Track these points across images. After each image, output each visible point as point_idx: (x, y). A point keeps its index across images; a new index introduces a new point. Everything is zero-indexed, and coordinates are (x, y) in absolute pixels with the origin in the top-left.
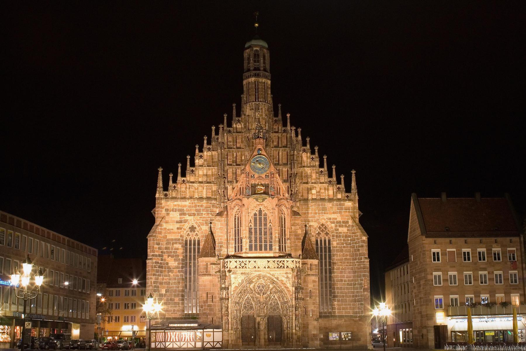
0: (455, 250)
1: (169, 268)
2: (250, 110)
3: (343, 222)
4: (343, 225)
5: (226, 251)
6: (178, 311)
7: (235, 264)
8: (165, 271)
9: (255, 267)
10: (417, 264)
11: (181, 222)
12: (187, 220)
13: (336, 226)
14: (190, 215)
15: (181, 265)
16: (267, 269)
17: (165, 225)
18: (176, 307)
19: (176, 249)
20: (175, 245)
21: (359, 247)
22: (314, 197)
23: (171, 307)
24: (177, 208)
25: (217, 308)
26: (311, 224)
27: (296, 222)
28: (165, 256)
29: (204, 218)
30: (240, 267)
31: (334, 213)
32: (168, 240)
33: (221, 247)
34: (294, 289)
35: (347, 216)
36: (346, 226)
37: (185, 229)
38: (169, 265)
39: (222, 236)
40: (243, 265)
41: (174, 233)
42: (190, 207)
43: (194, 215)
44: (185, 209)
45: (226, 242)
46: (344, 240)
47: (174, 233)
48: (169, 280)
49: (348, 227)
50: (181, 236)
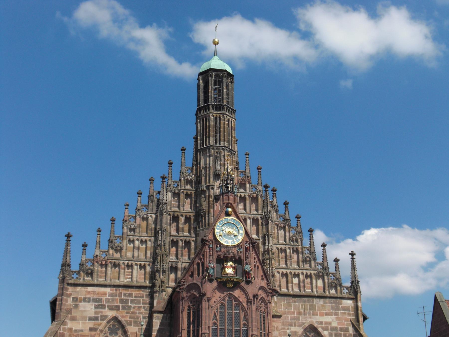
3: (341, 329)
11: (96, 319)
12: (106, 316)
14: (111, 308)
17: (70, 324)
22: (296, 290)
24: (91, 296)
26: (293, 329)
27: (275, 324)
29: (133, 313)
31: (327, 314)
35: (346, 320)
37: (101, 331)
42: (111, 295)
43: (117, 308)
44: (104, 298)
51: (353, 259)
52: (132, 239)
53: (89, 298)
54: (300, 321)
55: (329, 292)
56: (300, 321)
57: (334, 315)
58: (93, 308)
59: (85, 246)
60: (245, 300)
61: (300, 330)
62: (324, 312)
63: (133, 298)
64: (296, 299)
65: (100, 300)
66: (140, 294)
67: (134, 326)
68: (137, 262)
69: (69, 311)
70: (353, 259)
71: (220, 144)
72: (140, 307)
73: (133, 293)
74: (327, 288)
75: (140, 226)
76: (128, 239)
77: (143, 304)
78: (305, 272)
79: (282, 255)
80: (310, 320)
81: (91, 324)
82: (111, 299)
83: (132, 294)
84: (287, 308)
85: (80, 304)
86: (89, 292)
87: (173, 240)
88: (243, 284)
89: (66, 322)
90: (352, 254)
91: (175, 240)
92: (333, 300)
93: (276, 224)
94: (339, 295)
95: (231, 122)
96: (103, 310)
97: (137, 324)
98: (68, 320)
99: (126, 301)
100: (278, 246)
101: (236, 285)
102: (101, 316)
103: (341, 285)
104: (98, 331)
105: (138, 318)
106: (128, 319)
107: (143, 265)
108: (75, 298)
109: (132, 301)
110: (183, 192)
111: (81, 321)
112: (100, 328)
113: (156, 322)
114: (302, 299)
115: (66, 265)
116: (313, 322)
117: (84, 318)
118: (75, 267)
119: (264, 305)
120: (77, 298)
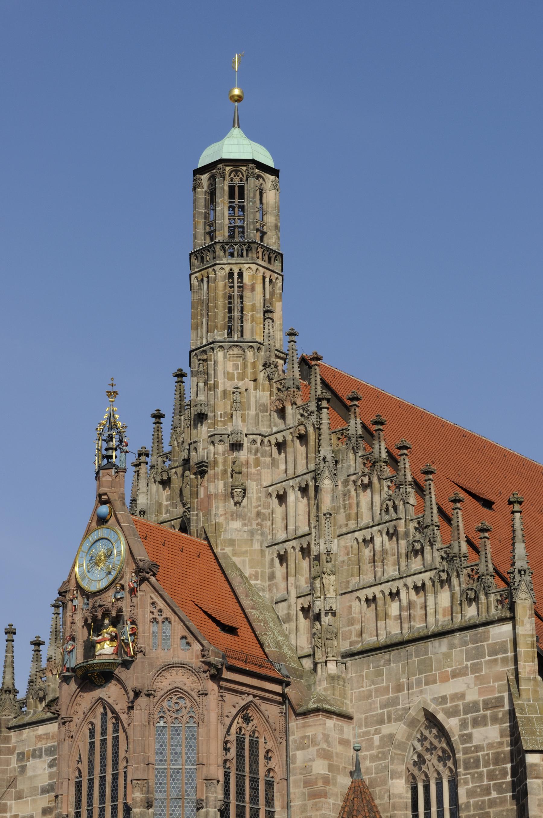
3: (487, 705)
4: (484, 717)
13: (464, 724)
26: (386, 729)
27: (310, 732)
31: (455, 675)
35: (497, 678)
36: (495, 719)
46: (491, 776)
49: (502, 721)
53: (41, 749)
54: (400, 707)
56: (400, 707)
57: (472, 673)
58: (47, 767)
59: (38, 644)
61: (398, 729)
62: (450, 669)
64: (393, 653)
69: (12, 783)
78: (410, 581)
79: (367, 552)
80: (420, 698)
84: (373, 683)
85: (28, 763)
86: (39, 738)
89: (5, 805)
92: (468, 634)
93: (353, 481)
94: (484, 617)
95: (241, 275)
98: (10, 800)
100: (357, 534)
110: (176, 473)
111: (29, 799)
114: (403, 652)
116: (425, 702)
119: (189, 704)
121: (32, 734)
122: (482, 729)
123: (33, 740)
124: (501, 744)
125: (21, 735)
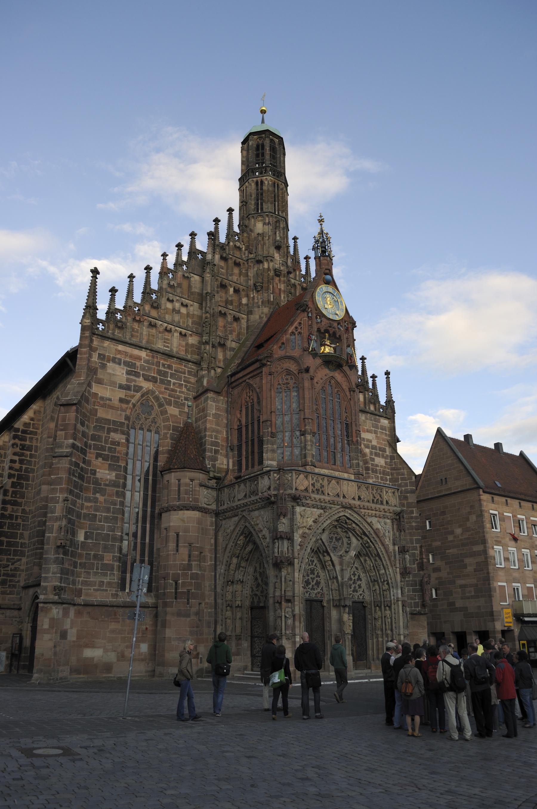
0: (510, 515)
1: (96, 482)
2: (264, 224)
3: (380, 449)
4: (379, 453)
5: (225, 462)
6: (110, 584)
7: (306, 483)
8: (87, 489)
9: (338, 495)
10: (452, 532)
12: (141, 388)
13: (371, 453)
14: (147, 379)
15: (122, 481)
16: (357, 503)
18: (105, 575)
19: (113, 443)
20: (112, 434)
21: (408, 492)
23: (96, 574)
25: (207, 583)
28: (91, 456)
29: (173, 390)
30: (313, 492)
32: (99, 420)
33: (216, 452)
34: (397, 548)
35: (384, 440)
36: (383, 457)
38: (98, 475)
39: (217, 431)
40: (318, 486)
41: (112, 407)
42: (146, 361)
43: (154, 380)
44: (138, 364)
45: (224, 444)
46: (382, 479)
47: (112, 407)
48: (96, 510)
50: (127, 418)
51: (388, 378)
52: (171, 299)
53: (120, 360)
55: (369, 408)
60: (348, 390)
63: (173, 372)
65: (134, 365)
66: (181, 368)
67: (174, 407)
68: (177, 328)
70: (388, 378)
71: (278, 213)
72: (181, 385)
73: (173, 365)
74: (367, 404)
75: (180, 285)
76: (167, 298)
77: (184, 382)
81: (122, 394)
82: (147, 367)
83: (172, 366)
85: (108, 364)
86: (120, 352)
87: (220, 312)
88: (346, 368)
90: (387, 373)
91: (223, 312)
92: (373, 417)
94: (377, 412)
96: (137, 379)
97: (178, 405)
99: (165, 374)
101: (339, 366)
102: (135, 386)
103: (379, 402)
104: (131, 405)
105: (179, 397)
106: (168, 397)
107: (183, 333)
108: (102, 354)
109: (172, 376)
111: (109, 387)
112: (133, 401)
113: (211, 405)
115: (91, 308)
117: (113, 384)
118: (101, 315)
120: (104, 356)
121: (112, 346)
122: (378, 458)
123: (114, 351)
124: (385, 467)
125: (104, 343)
